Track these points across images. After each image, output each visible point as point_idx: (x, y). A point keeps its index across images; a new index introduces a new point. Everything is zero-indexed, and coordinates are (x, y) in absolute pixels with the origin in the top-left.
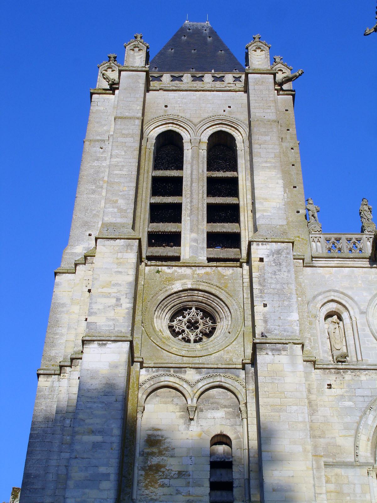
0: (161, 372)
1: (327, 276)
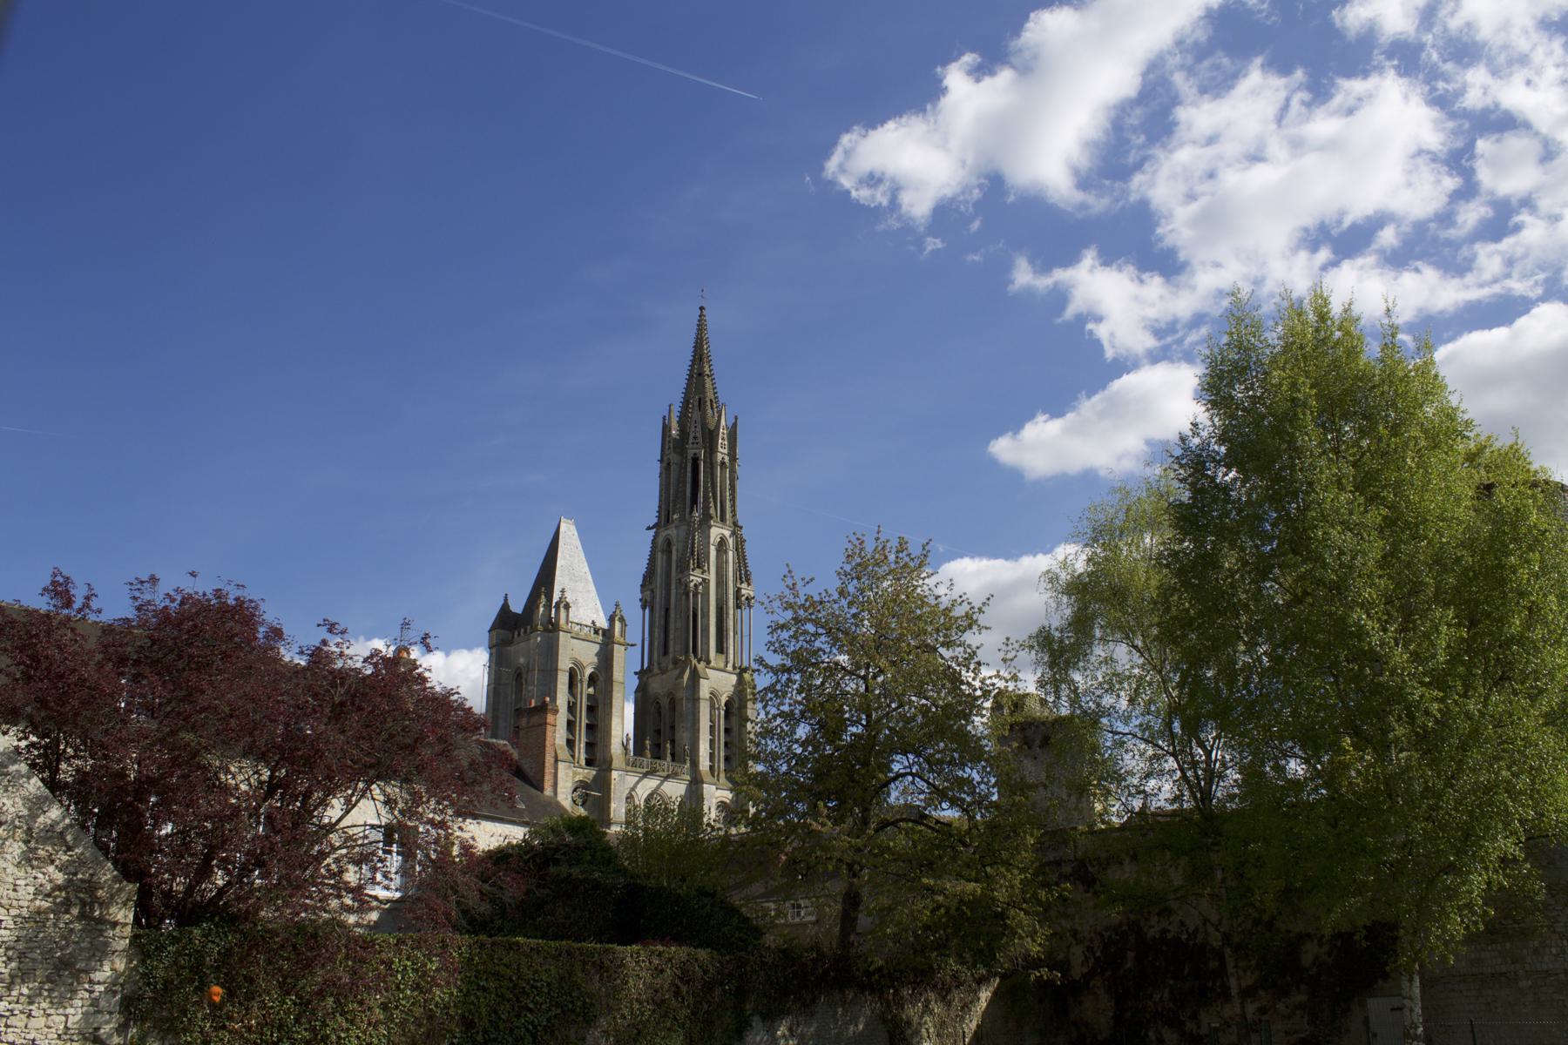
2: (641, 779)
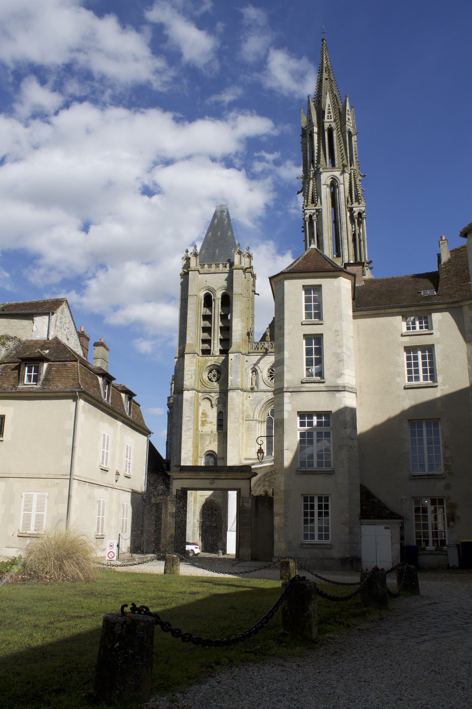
0: (205, 394)
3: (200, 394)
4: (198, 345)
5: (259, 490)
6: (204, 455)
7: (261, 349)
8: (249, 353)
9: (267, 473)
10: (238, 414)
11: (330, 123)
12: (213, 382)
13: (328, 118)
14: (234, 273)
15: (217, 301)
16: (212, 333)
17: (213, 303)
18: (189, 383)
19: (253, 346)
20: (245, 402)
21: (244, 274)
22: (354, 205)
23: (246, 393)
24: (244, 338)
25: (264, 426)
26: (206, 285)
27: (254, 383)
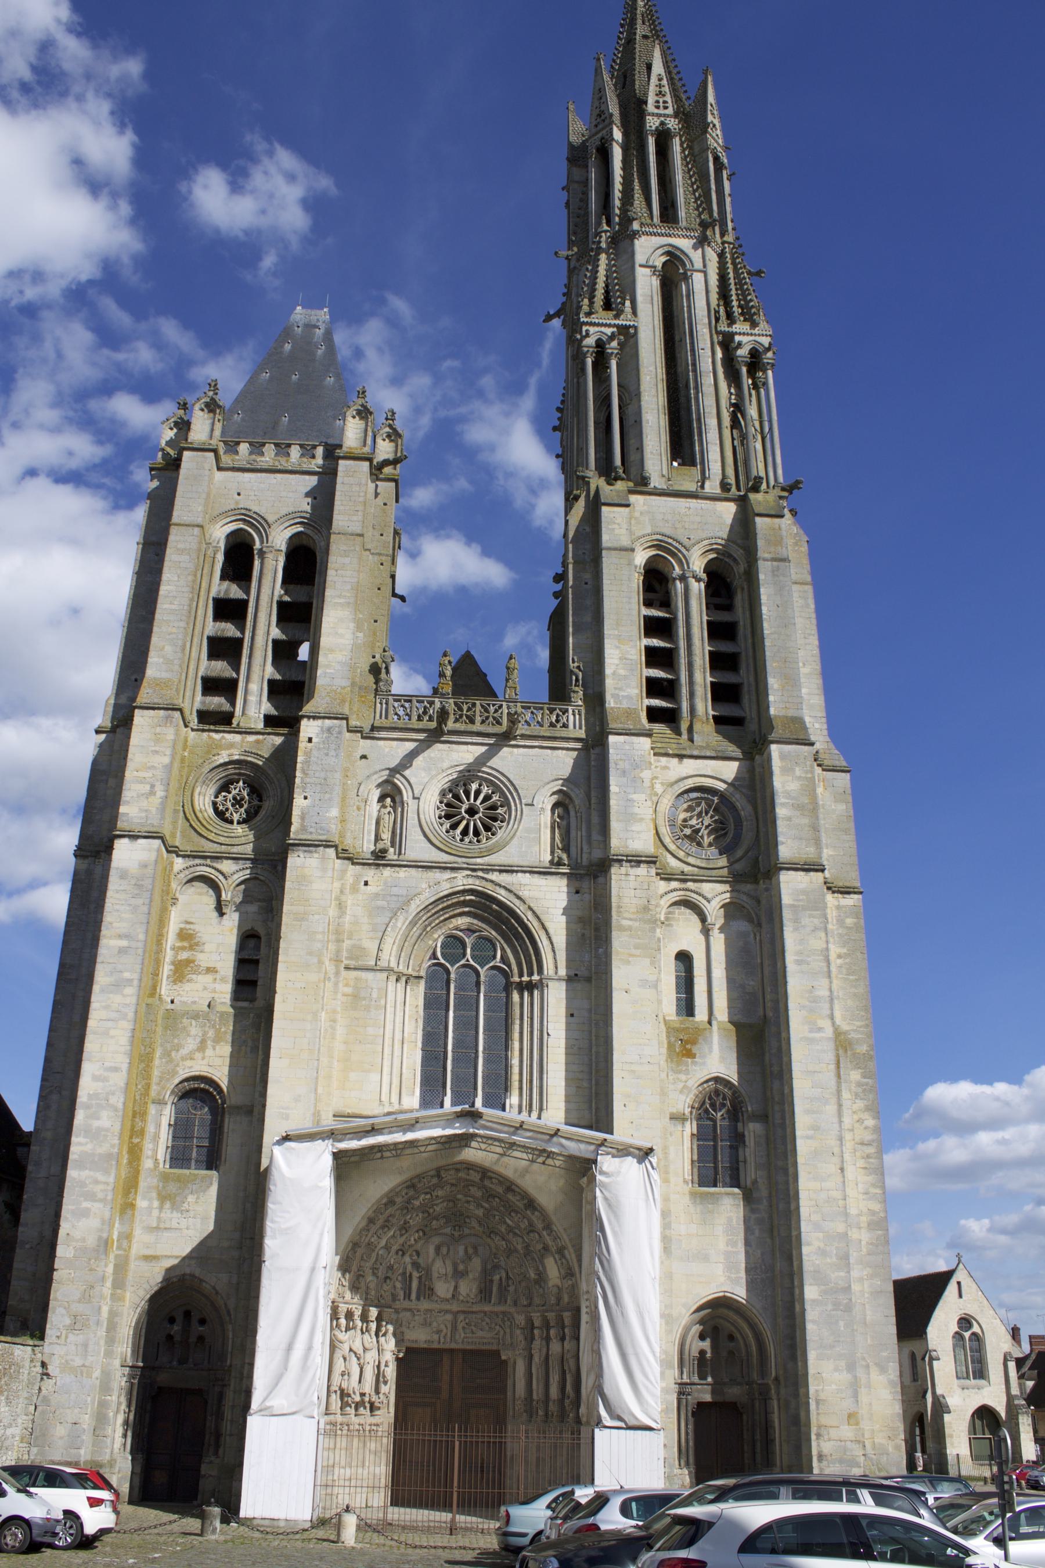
0: (198, 861)
1: (387, 750)
2: (424, 746)
3: (179, 863)
4: (188, 694)
5: (383, 1243)
6: (172, 1092)
7: (420, 718)
8: (373, 728)
9: (419, 1177)
10: (319, 937)
11: (662, 119)
12: (231, 822)
13: (658, 107)
14: (340, 468)
15: (270, 557)
16: (244, 660)
17: (257, 563)
18: (141, 810)
19: (391, 709)
20: (349, 900)
21: (373, 481)
22: (737, 327)
23: (352, 870)
24: (357, 680)
25: (417, 994)
26: (237, 503)
27: (386, 836)
